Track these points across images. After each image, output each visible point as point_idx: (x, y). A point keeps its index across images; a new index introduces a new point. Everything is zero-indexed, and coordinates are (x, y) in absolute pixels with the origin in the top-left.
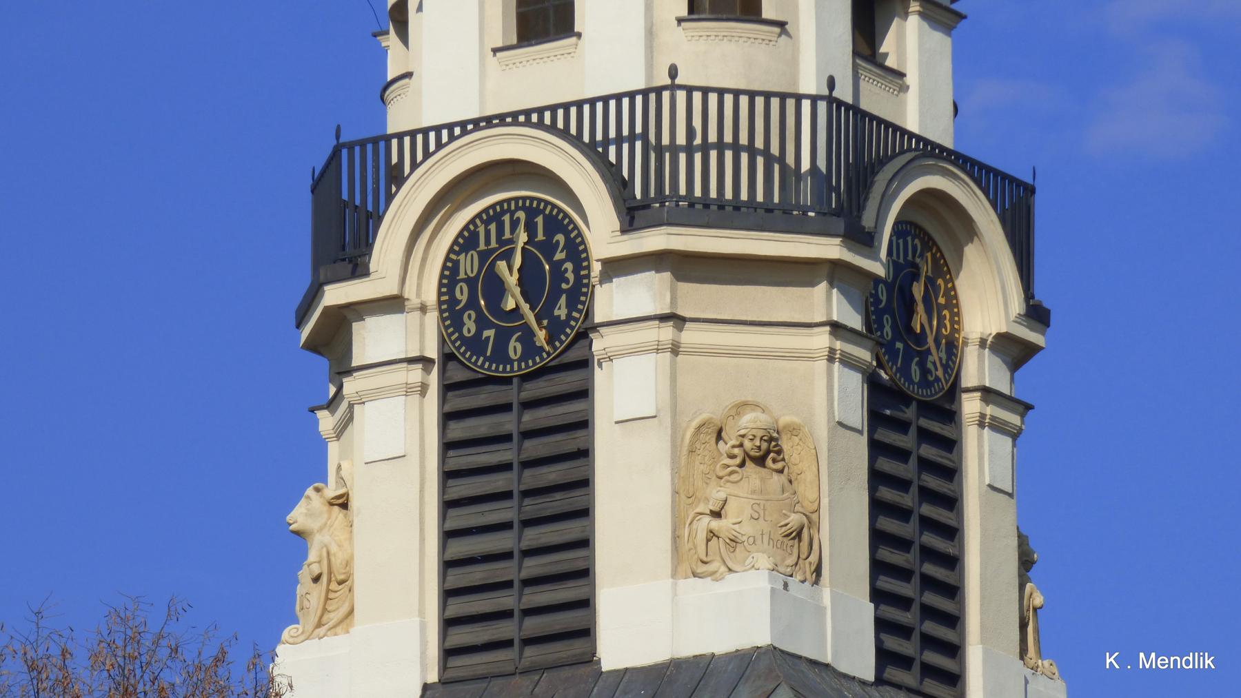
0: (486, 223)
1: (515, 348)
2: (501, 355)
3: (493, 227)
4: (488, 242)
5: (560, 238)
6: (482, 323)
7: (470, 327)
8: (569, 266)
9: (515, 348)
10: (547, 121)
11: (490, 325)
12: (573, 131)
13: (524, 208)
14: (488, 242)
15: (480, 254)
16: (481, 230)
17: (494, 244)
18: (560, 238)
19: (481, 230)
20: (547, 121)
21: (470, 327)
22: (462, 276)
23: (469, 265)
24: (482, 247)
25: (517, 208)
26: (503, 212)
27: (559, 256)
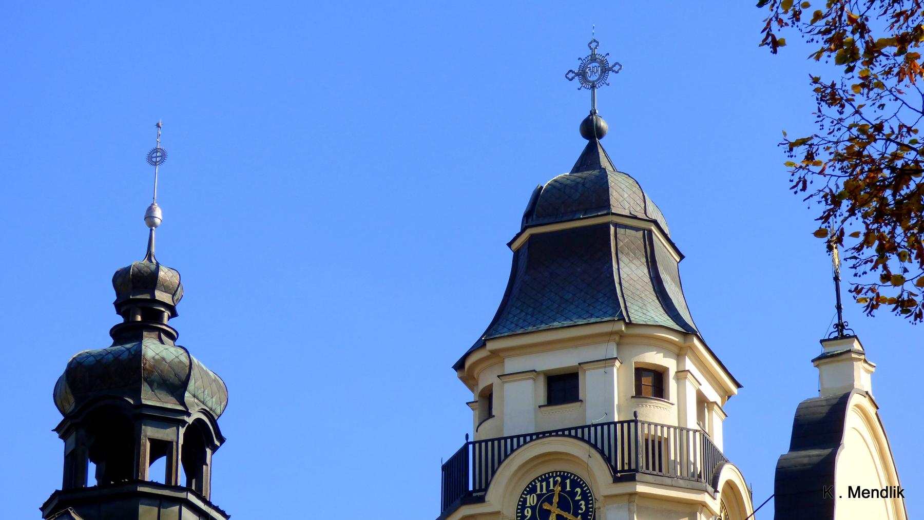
0: (541, 482)
3: (544, 484)
4: (541, 489)
8: (583, 502)
10: (580, 435)
12: (593, 441)
13: (560, 476)
14: (541, 489)
15: (538, 495)
16: (538, 484)
17: (544, 491)
18: (578, 490)
19: (538, 484)
20: (580, 435)
22: (528, 505)
23: (531, 500)
24: (539, 492)
25: (557, 476)
26: (550, 477)
27: (578, 498)
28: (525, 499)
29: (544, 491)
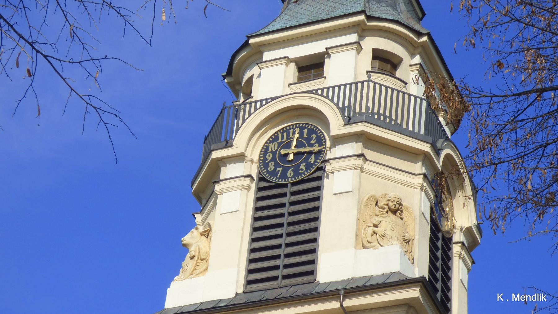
0: (282, 133)
1: (290, 173)
2: (284, 175)
3: (285, 134)
5: (314, 136)
6: (277, 165)
7: (271, 167)
9: (290, 173)
11: (280, 166)
13: (299, 127)
16: (280, 135)
17: (285, 139)
18: (314, 136)
19: (280, 135)
21: (271, 167)
22: (270, 150)
24: (280, 140)
25: (296, 127)
26: (290, 129)
27: (312, 142)
28: (268, 147)
29: (285, 139)
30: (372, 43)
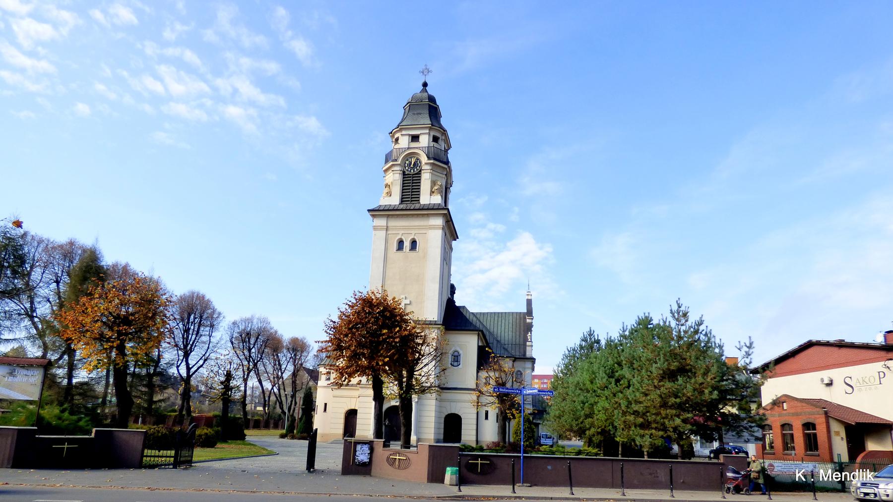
30: (432, 133)
